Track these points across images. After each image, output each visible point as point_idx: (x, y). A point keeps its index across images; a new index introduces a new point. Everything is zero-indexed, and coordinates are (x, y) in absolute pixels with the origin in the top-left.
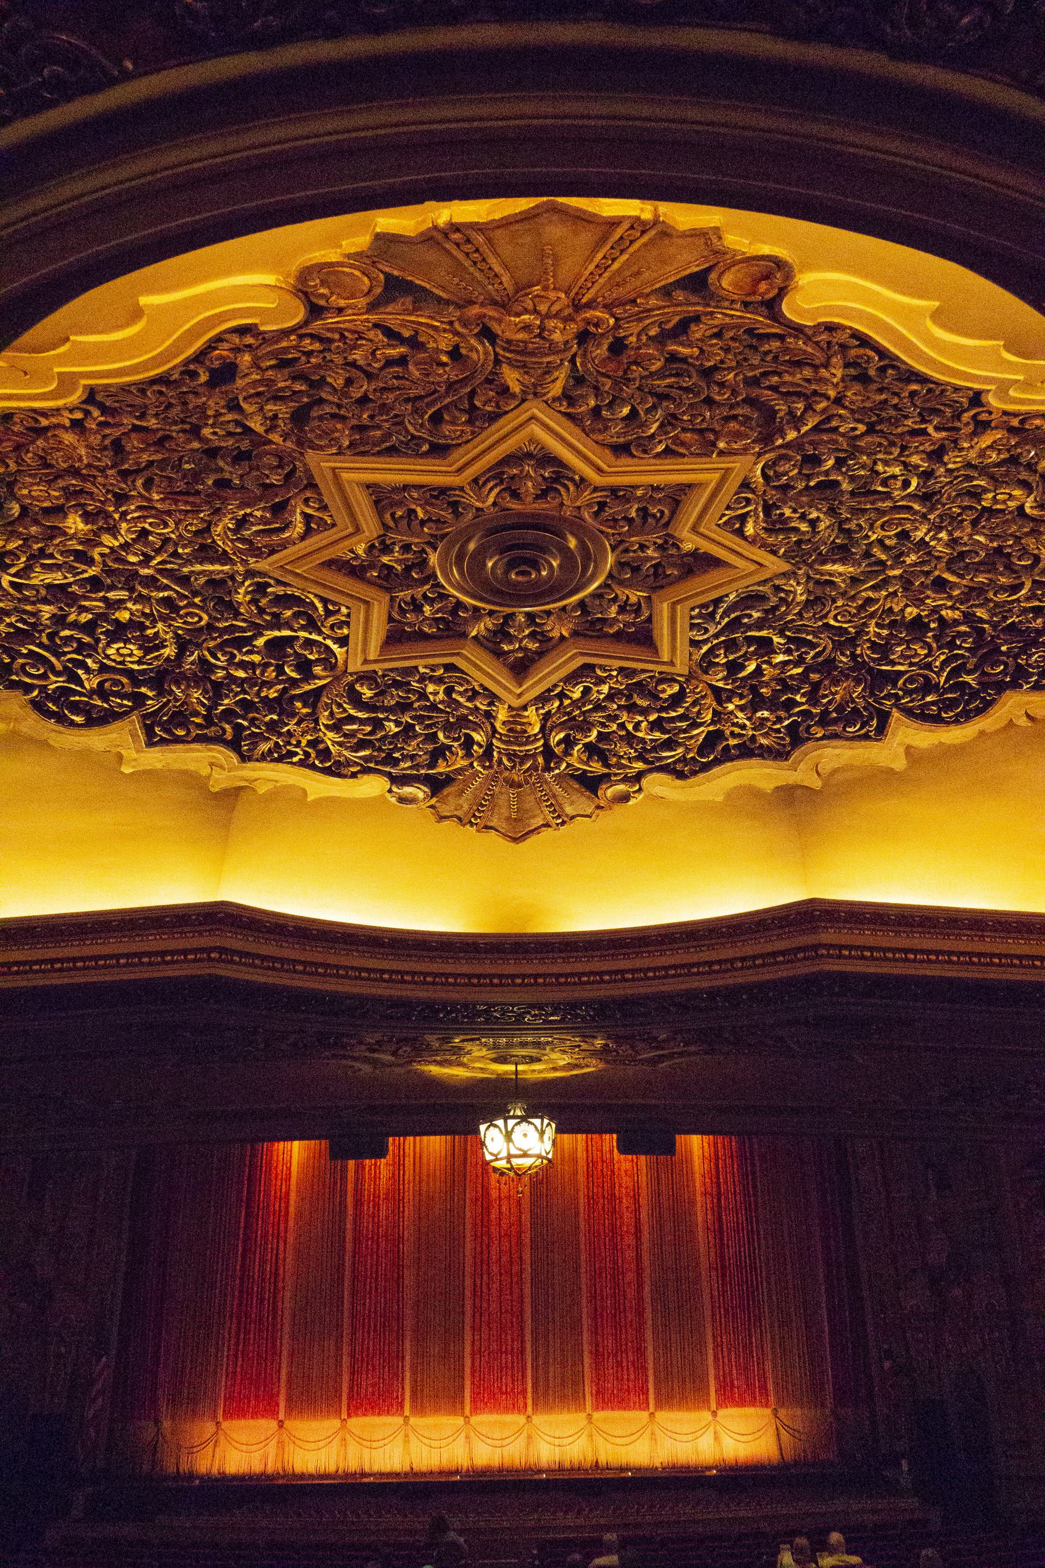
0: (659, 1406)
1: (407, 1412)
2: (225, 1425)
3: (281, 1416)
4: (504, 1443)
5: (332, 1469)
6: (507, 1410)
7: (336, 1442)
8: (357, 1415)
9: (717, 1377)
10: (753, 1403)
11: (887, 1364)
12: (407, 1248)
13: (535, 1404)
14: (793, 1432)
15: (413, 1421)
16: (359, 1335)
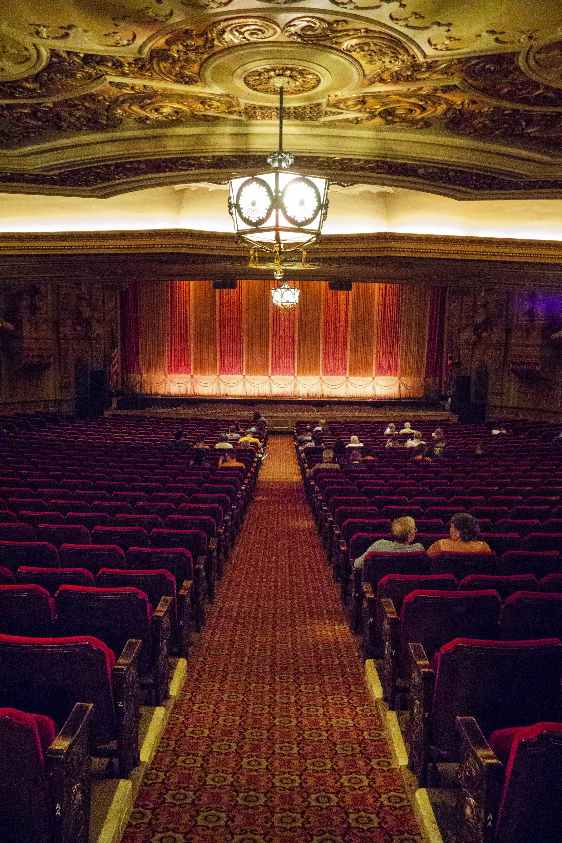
0: (351, 374)
1: (244, 373)
2: (169, 376)
3: (192, 373)
5: (214, 393)
6: (286, 374)
7: (215, 384)
9: (376, 364)
10: (391, 374)
11: (450, 362)
12: (244, 309)
13: (298, 371)
14: (406, 386)
15: (247, 377)
16: (223, 343)
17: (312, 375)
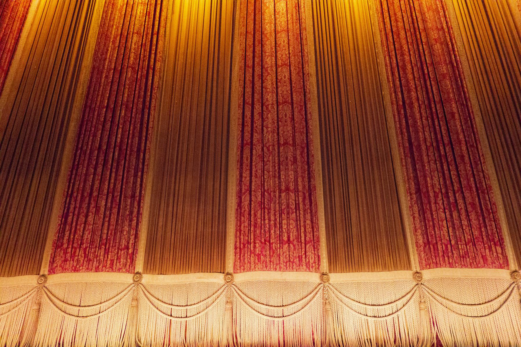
1: (139, 266)
4: (287, 310)
6: (290, 264)
8: (64, 270)
15: (147, 279)
17: (385, 267)
